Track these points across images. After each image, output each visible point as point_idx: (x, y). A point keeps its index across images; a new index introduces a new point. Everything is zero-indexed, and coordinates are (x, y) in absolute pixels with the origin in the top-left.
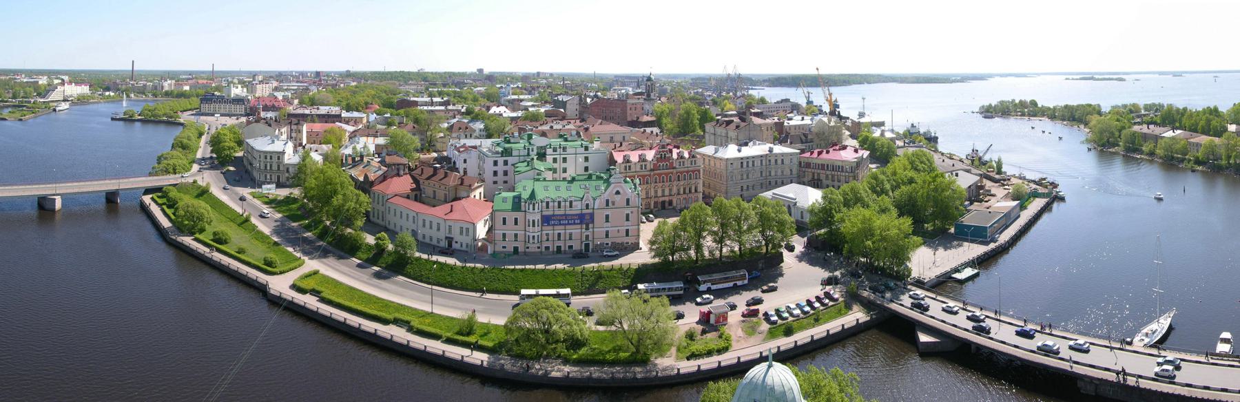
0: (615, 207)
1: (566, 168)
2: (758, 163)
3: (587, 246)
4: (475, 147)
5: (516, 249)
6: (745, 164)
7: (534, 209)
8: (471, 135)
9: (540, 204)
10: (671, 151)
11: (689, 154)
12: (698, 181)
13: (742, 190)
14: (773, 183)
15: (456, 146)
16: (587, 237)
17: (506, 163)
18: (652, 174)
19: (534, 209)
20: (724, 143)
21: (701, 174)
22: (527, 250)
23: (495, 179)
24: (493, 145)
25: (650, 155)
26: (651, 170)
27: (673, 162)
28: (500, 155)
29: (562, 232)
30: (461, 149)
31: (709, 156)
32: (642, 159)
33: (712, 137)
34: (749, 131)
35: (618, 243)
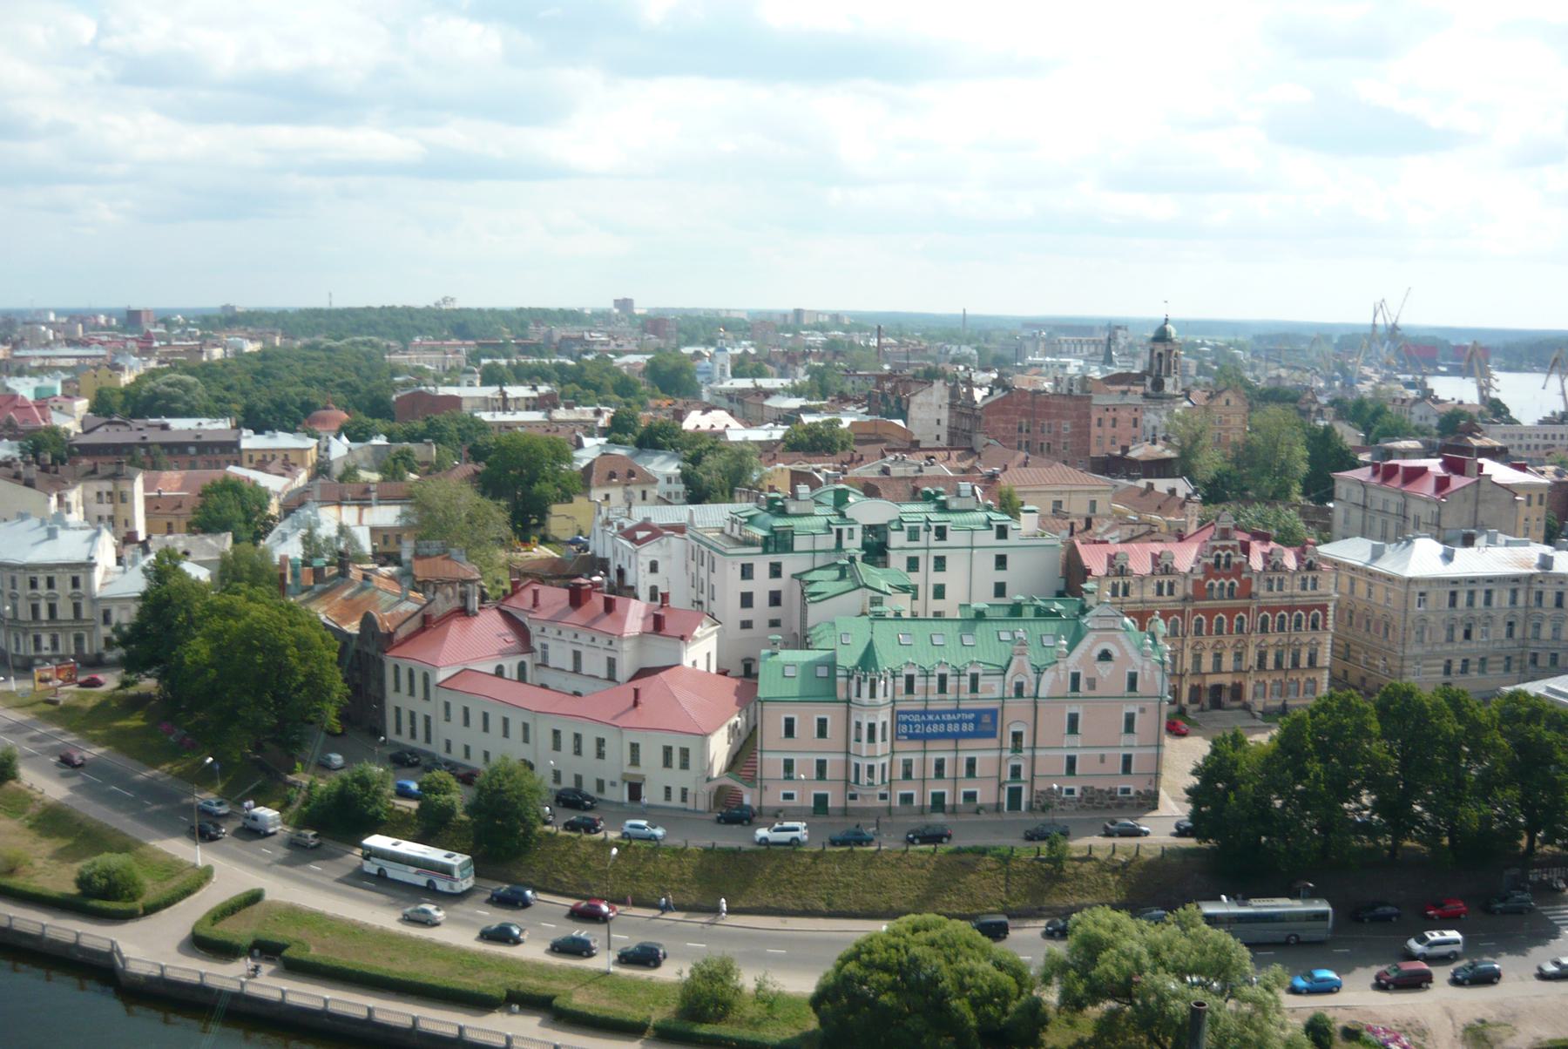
0: (1092, 693)
2: (1502, 598)
3: (1015, 794)
4: (679, 529)
5: (821, 800)
6: (1462, 599)
8: (644, 493)
9: (890, 681)
10: (1246, 548)
11: (1299, 559)
13: (1448, 671)
14: (1544, 661)
15: (620, 527)
16: (1016, 771)
17: (776, 571)
18: (1189, 609)
19: (873, 695)
20: (1400, 531)
21: (1330, 617)
22: (851, 803)
23: (747, 614)
24: (733, 521)
25: (1186, 557)
26: (1185, 599)
27: (1250, 580)
29: (948, 757)
30: (640, 535)
31: (1353, 568)
32: (1162, 566)
33: (1357, 514)
34: (1477, 502)
35: (1101, 791)
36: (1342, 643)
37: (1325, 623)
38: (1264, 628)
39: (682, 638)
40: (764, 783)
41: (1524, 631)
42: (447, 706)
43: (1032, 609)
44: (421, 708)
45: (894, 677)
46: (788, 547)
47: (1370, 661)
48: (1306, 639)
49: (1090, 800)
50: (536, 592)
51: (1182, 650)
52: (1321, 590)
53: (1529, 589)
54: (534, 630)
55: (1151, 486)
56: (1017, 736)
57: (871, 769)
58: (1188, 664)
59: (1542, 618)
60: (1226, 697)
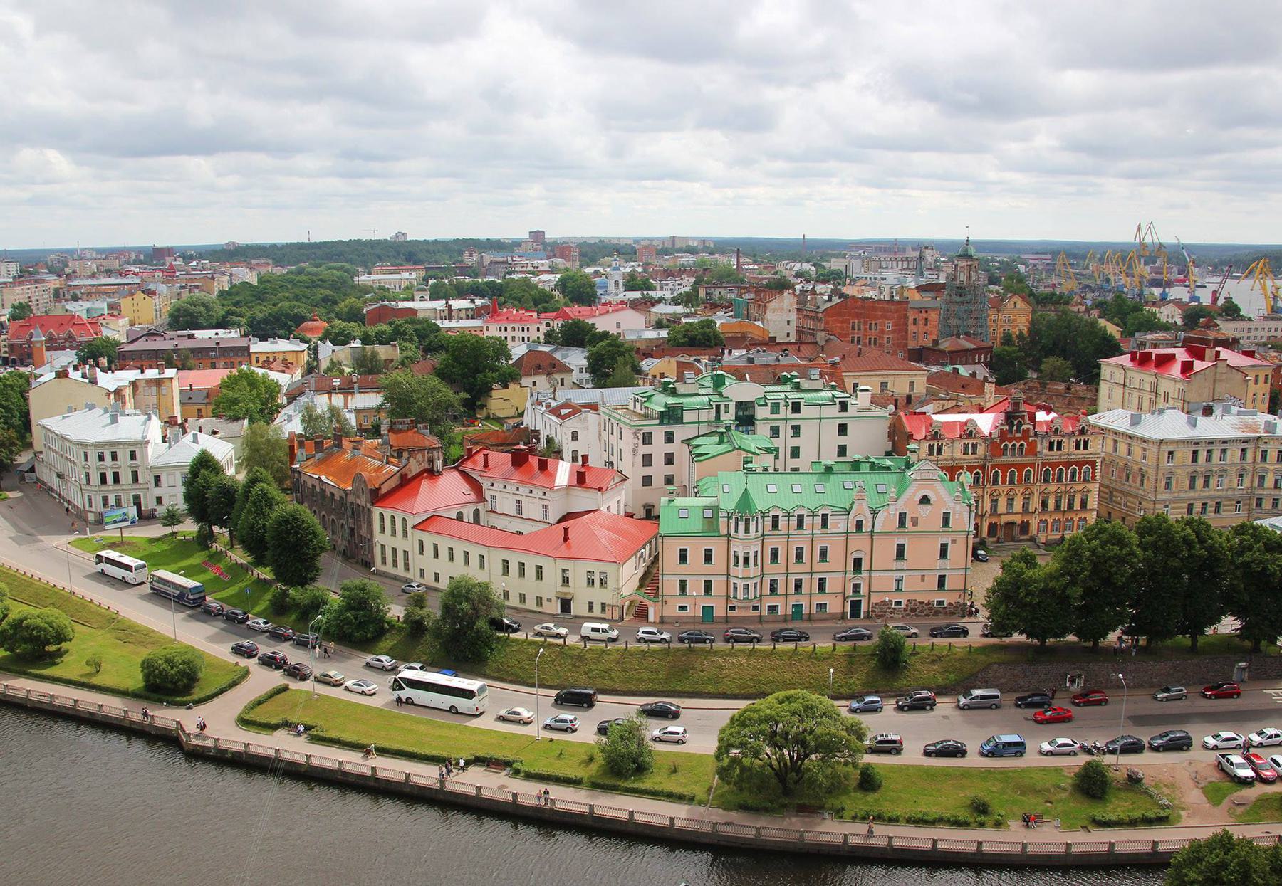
0: (915, 529)
1: (798, 448)
3: (856, 606)
4: (593, 407)
5: (708, 610)
6: (1202, 456)
7: (747, 530)
9: (760, 521)
12: (1090, 486)
15: (548, 406)
16: (856, 587)
17: (669, 438)
19: (747, 530)
22: (731, 613)
23: (648, 471)
24: (636, 400)
28: (657, 422)
30: (564, 412)
33: (1119, 390)
34: (1215, 381)
35: (921, 603)
36: (1107, 490)
37: (1093, 478)
38: (1046, 480)
39: (600, 489)
40: (665, 598)
41: (1252, 482)
42: (421, 543)
43: (868, 465)
44: (399, 543)
45: (763, 517)
46: (679, 420)
47: (1128, 504)
48: (1079, 488)
49: (913, 610)
50: (486, 456)
51: (983, 496)
52: (1090, 450)
53: (1257, 447)
54: (486, 484)
55: (956, 371)
56: (858, 563)
57: (746, 587)
58: (987, 506)
59: (1266, 471)
60: (1016, 531)
